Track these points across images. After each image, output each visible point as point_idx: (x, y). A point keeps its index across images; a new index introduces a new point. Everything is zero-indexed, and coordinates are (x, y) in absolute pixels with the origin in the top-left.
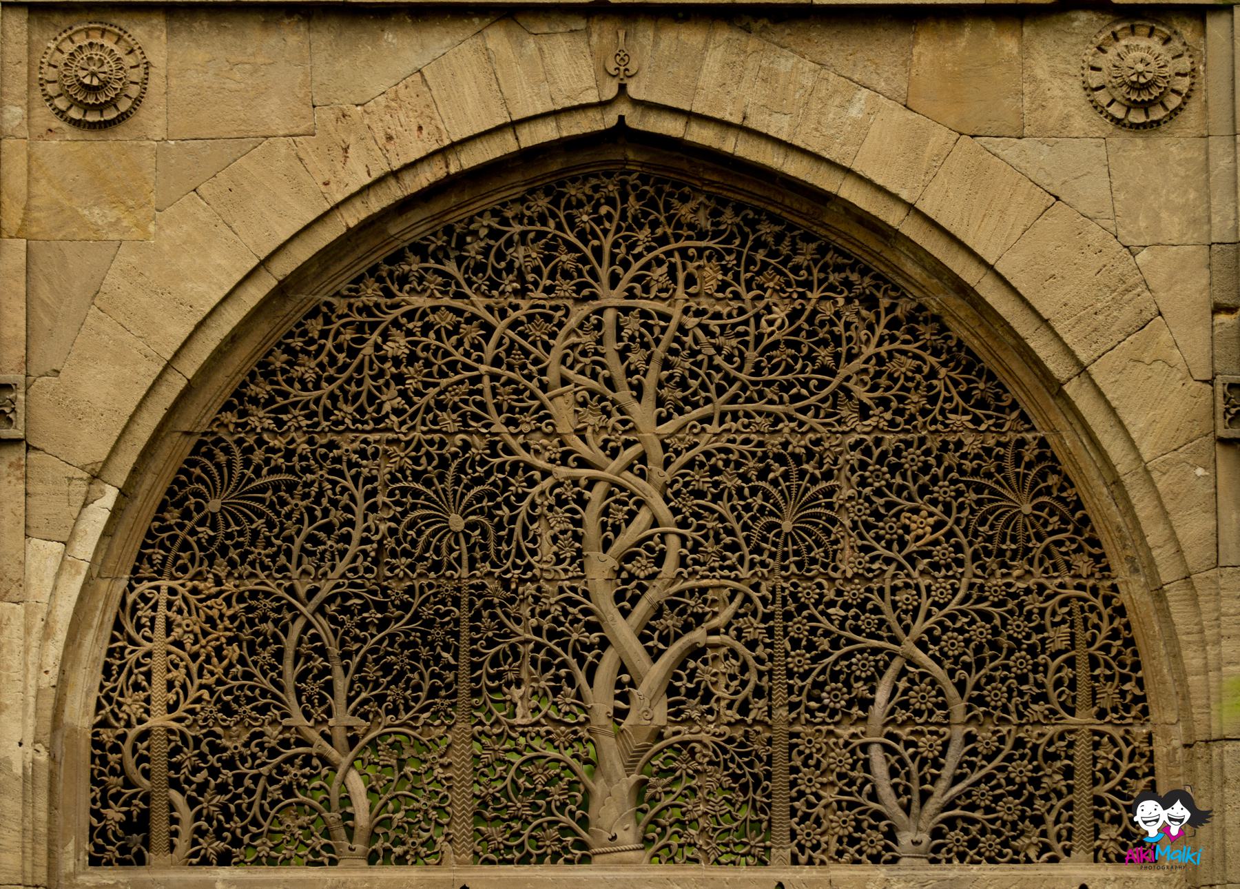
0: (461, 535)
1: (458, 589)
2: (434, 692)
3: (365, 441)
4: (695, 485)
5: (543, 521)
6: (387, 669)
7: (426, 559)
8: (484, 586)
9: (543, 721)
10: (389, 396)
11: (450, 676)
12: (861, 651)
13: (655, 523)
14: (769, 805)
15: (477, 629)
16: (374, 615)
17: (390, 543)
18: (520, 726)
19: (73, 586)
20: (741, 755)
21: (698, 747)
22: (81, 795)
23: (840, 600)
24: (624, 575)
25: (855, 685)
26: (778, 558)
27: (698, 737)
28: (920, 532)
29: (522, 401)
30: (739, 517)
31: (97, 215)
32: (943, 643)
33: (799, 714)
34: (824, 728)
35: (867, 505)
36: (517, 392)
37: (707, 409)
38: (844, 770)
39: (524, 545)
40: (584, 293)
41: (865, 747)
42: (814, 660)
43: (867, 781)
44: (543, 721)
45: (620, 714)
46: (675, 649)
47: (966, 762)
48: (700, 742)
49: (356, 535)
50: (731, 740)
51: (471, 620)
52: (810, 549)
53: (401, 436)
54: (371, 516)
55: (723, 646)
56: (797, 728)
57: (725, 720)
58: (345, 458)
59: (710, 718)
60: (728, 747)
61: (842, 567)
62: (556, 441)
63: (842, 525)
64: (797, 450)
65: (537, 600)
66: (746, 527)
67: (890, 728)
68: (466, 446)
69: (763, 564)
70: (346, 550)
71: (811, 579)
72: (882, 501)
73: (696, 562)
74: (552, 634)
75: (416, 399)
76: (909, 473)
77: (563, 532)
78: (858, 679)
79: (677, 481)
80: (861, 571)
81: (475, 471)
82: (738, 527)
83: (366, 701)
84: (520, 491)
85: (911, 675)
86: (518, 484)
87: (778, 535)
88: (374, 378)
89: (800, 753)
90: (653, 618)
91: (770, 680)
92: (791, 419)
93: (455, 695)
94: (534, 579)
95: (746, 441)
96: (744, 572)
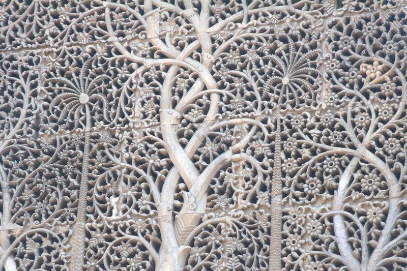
0: (87, 106)
1: (83, 140)
2: (64, 205)
3: (33, 55)
4: (230, 62)
5: (137, 94)
6: (37, 193)
7: (65, 123)
8: (98, 137)
9: (128, 216)
10: (50, 26)
11: (74, 193)
12: (330, 156)
13: (205, 88)
14: (268, 261)
15: (93, 164)
16: (31, 160)
17: (44, 114)
18: (114, 220)
20: (250, 229)
21: (223, 225)
23: (317, 124)
24: (184, 121)
25: (325, 178)
26: (280, 101)
27: (223, 219)
28: (372, 75)
29: (129, 21)
30: (256, 79)
32: (385, 146)
33: (288, 199)
34: (304, 208)
35: (338, 62)
36: (125, 16)
37: (238, 15)
38: (316, 234)
39: (125, 108)
41: (331, 219)
42: (300, 164)
43: (332, 240)
44: (128, 216)
45: (177, 209)
47: (400, 223)
48: (224, 222)
49: (24, 111)
50: (244, 220)
51: (91, 158)
52: (300, 94)
53: (54, 50)
54: (33, 98)
55: (242, 160)
56: (286, 209)
57: (240, 206)
58: (19, 66)
59: (231, 206)
60: (242, 224)
61: (319, 103)
62: (147, 44)
63: (321, 76)
64: (294, 33)
65: (130, 142)
66: (260, 85)
67: (347, 204)
68: (93, 52)
69: (270, 107)
70: (17, 122)
71: (300, 113)
72: (347, 58)
73: (228, 109)
74: (138, 163)
75: (64, 26)
76: (367, 38)
77: (148, 99)
78: (327, 174)
79: (218, 60)
80: (332, 104)
81: (97, 66)
82: (254, 85)
83: (22, 214)
84: (123, 76)
86: (123, 72)
87: (280, 88)
88: (40, 16)
89: (288, 225)
90: (200, 147)
91: (271, 178)
92: (291, 14)
93: (76, 205)
94: (128, 130)
95: (263, 31)
96: (258, 113)
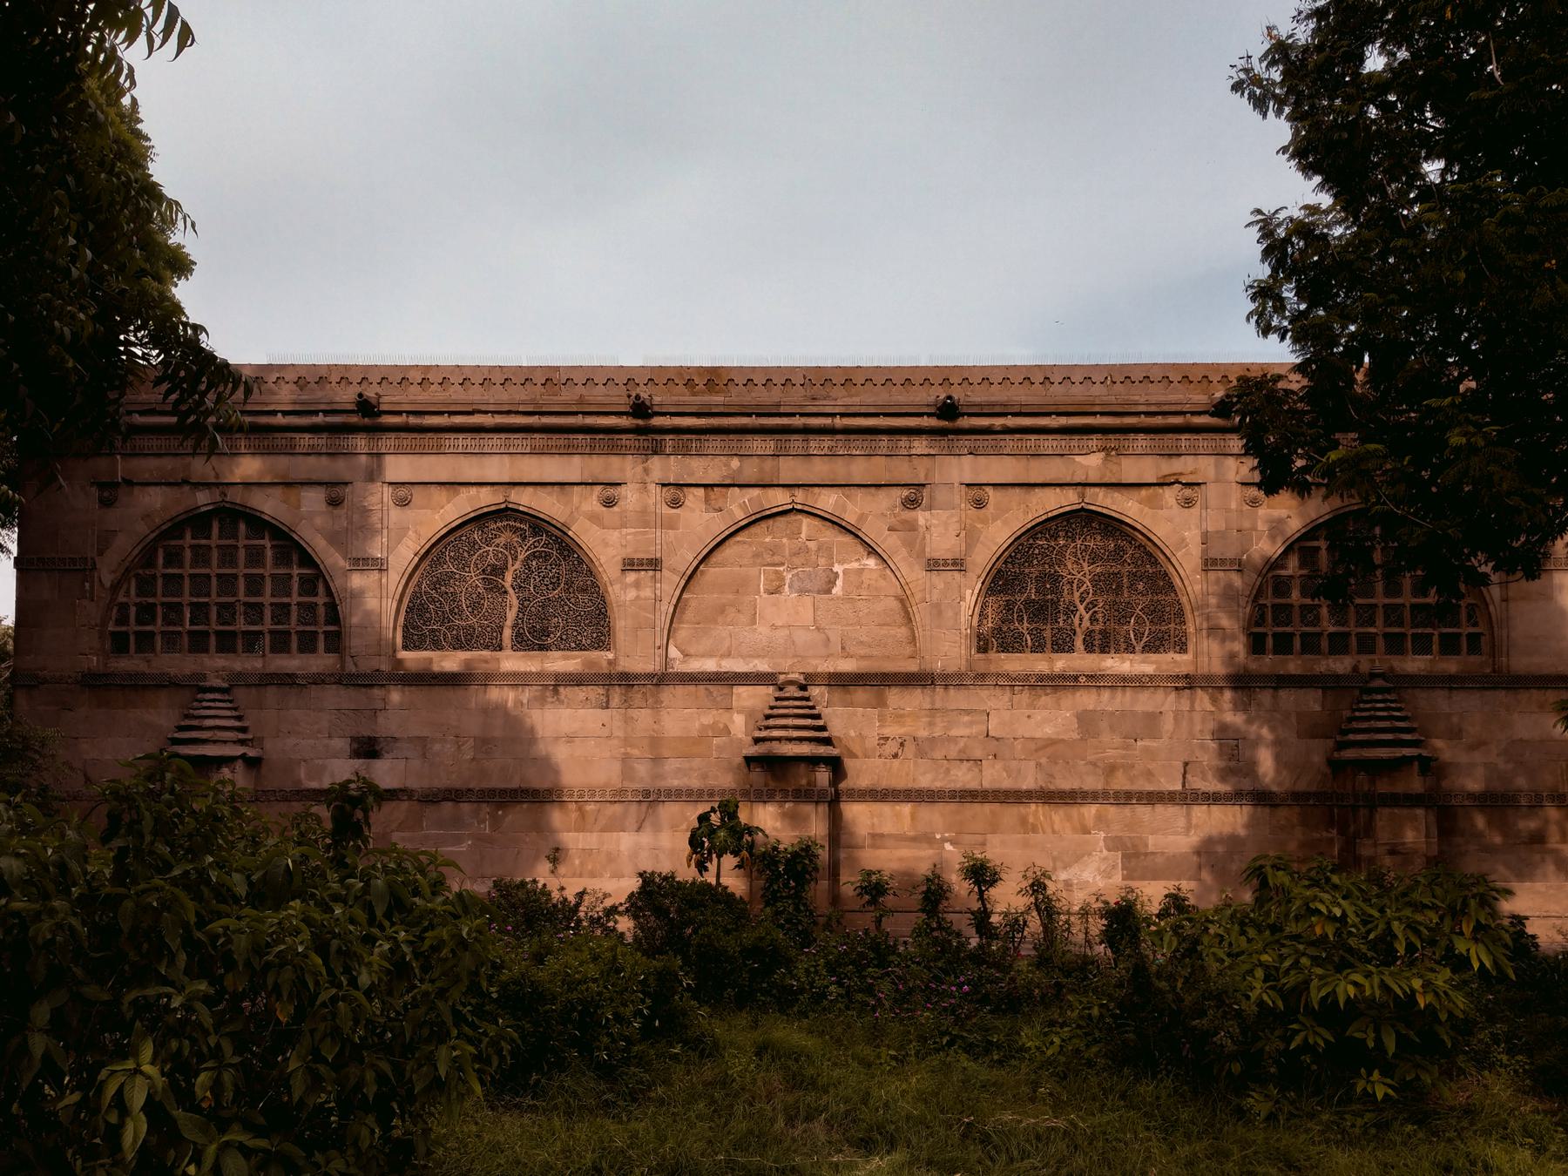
19: (974, 598)
22: (975, 640)
31: (979, 526)
40: (1073, 541)
46: (1091, 612)
85: (1139, 617)
